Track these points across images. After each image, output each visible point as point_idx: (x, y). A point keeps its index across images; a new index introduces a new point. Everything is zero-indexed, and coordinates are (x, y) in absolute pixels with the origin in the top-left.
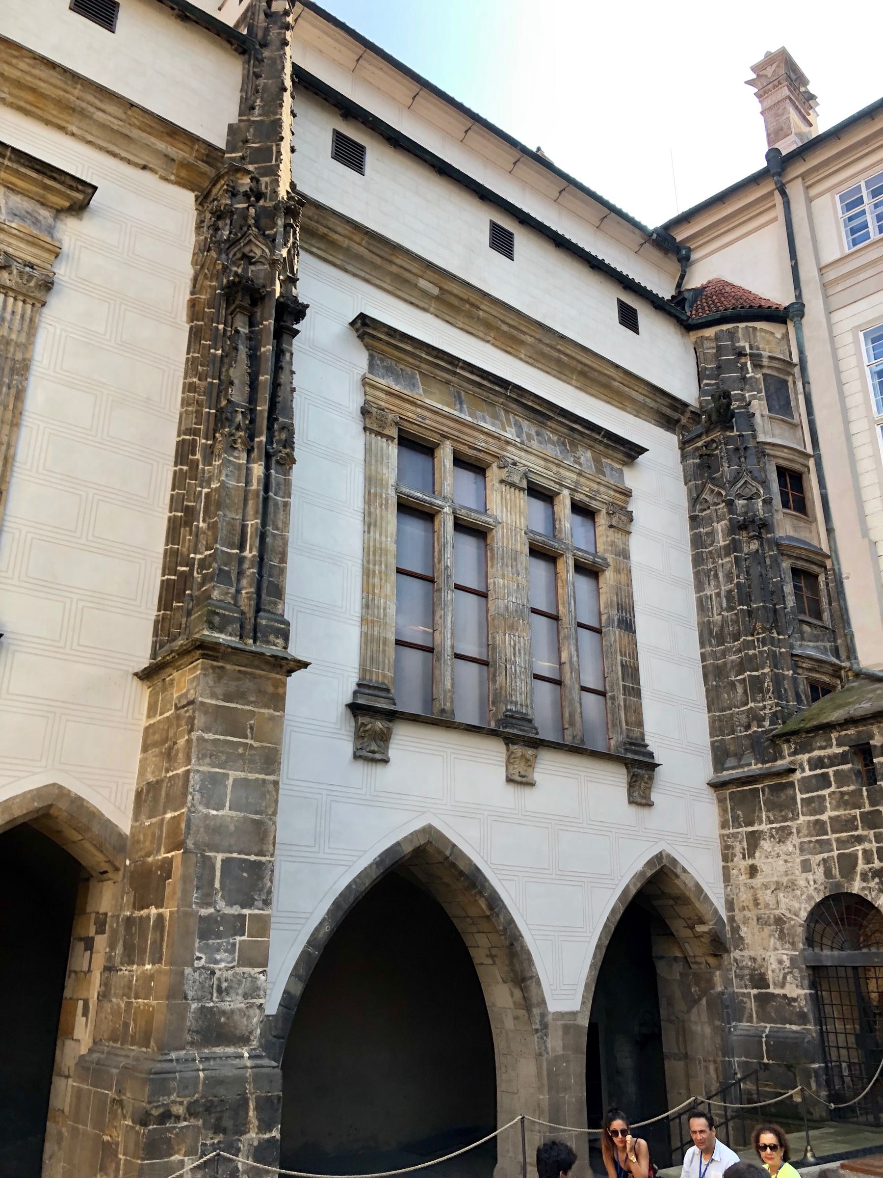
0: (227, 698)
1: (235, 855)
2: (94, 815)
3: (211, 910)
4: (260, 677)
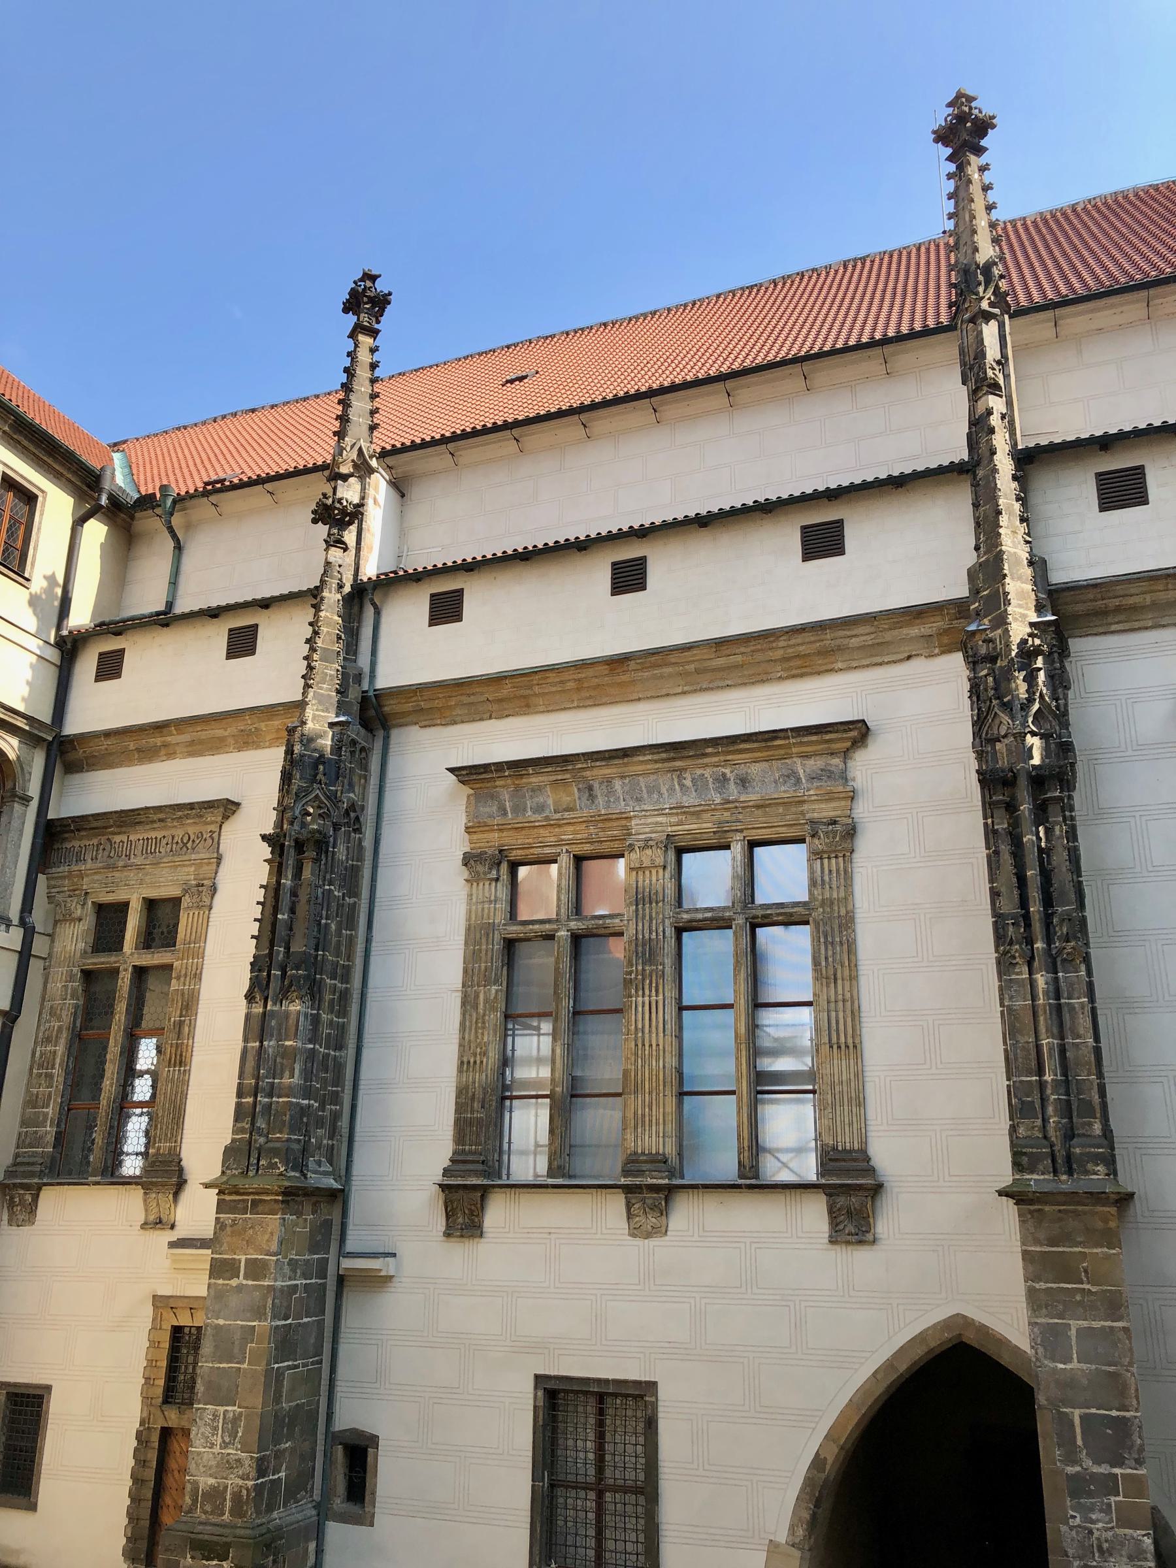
0: (1052, 1242)
1: (1094, 1411)
2: (1002, 1342)
3: (1078, 1469)
4: (1085, 1213)
